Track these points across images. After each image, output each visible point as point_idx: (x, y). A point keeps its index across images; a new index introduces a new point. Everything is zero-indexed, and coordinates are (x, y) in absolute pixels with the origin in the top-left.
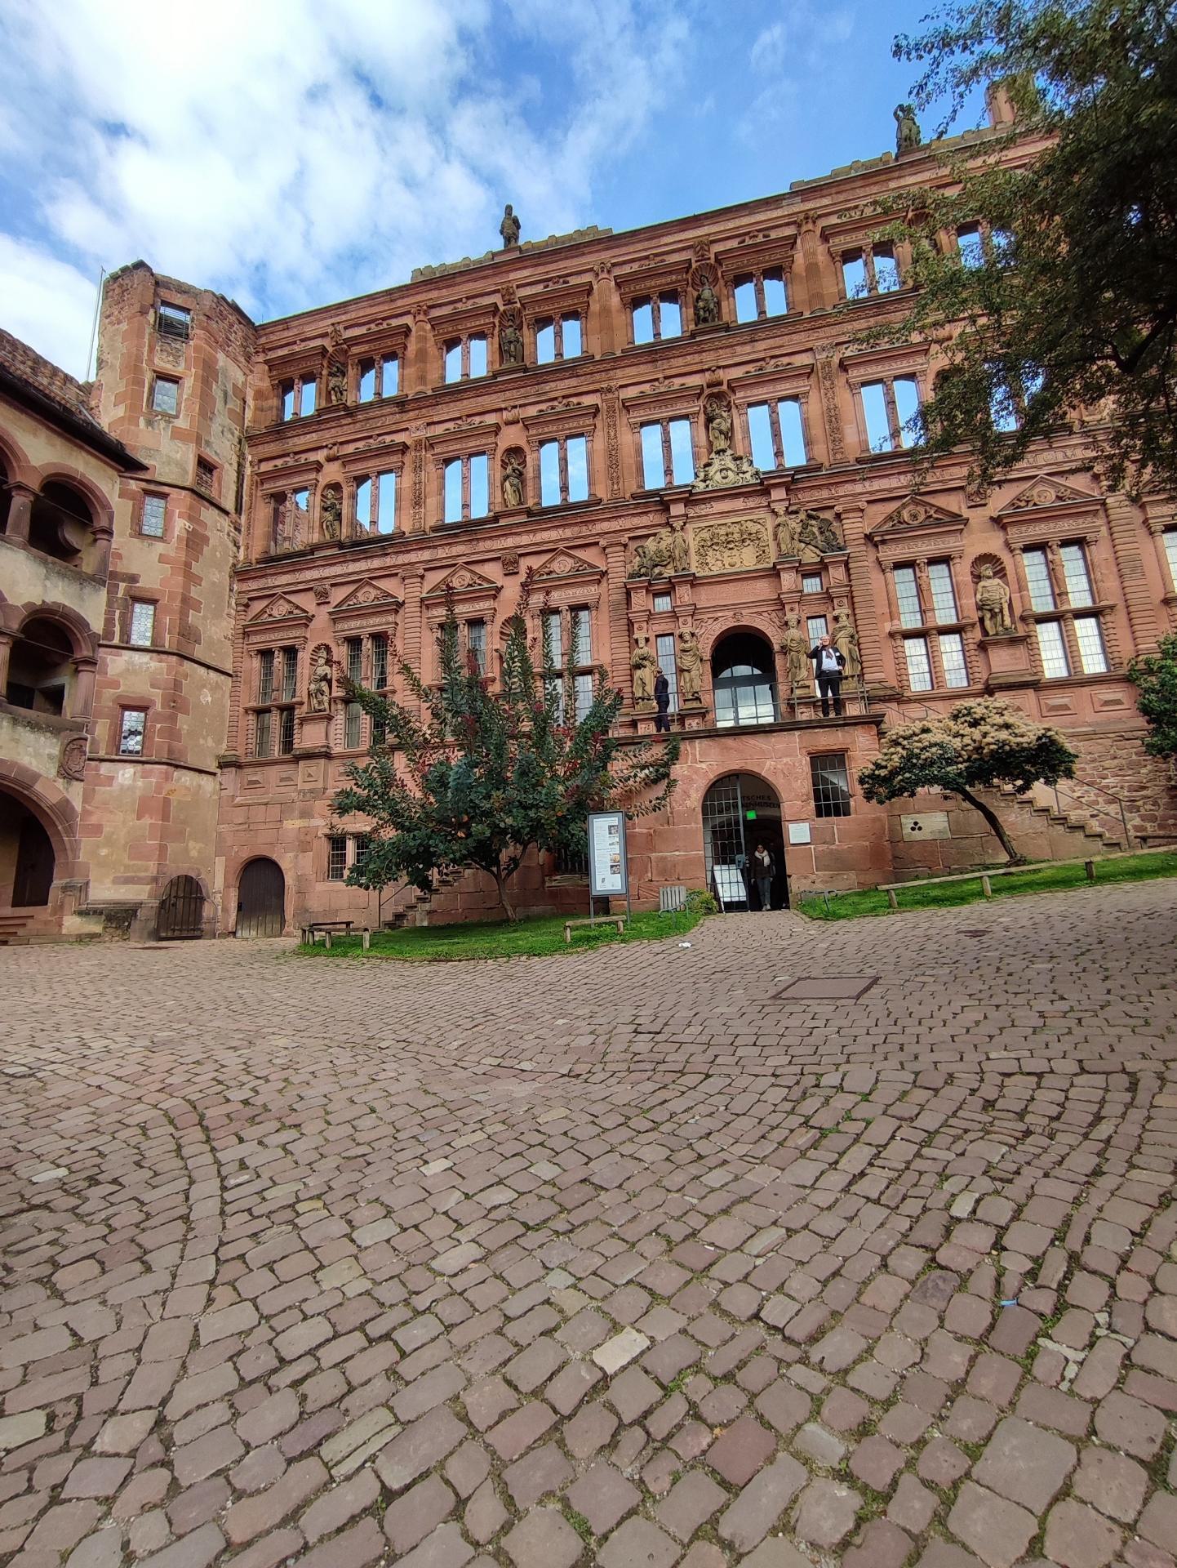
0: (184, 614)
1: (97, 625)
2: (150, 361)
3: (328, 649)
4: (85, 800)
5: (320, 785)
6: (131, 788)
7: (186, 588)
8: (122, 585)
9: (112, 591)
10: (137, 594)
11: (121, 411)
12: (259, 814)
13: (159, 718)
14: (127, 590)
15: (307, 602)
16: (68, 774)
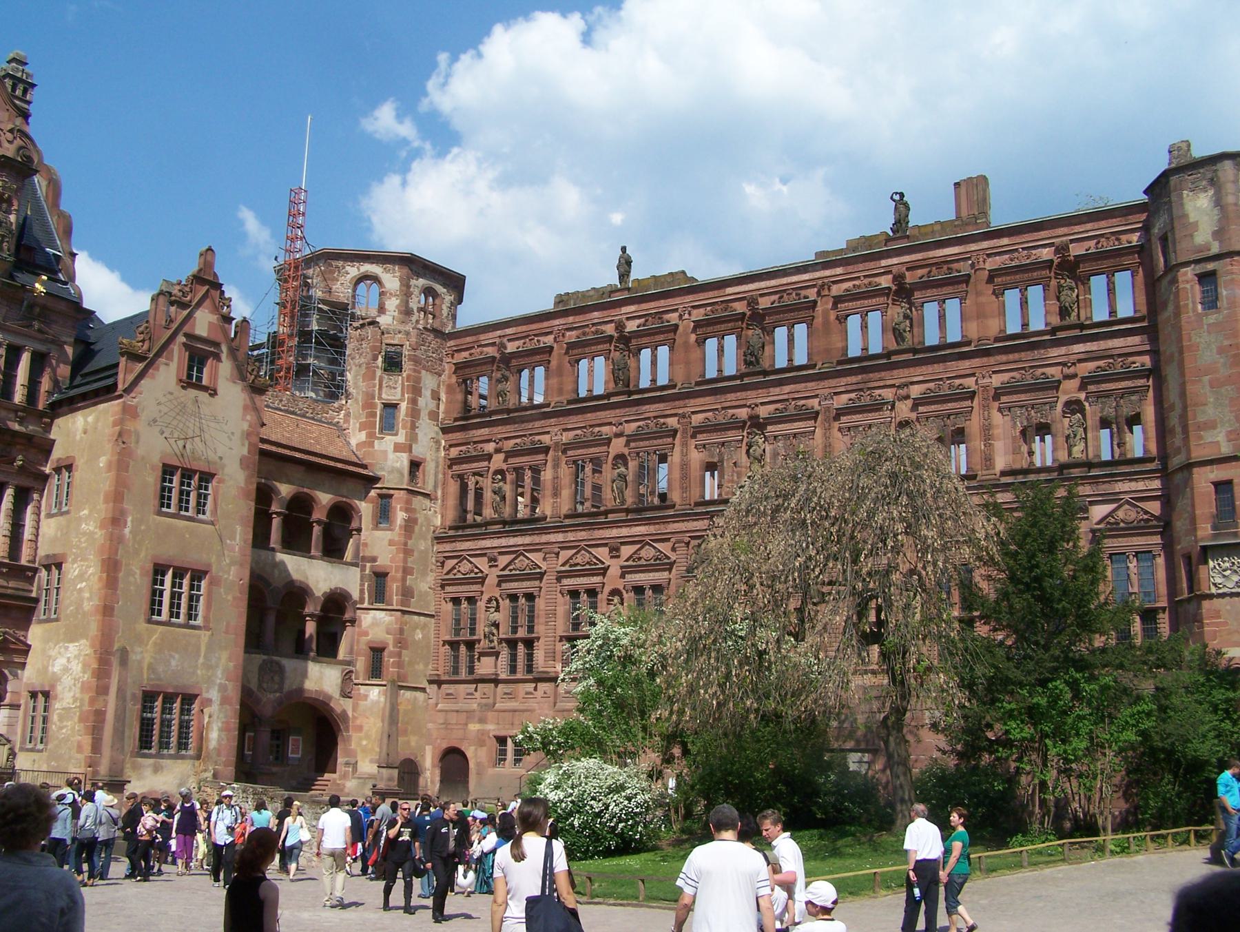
0: (404, 580)
1: (356, 595)
2: (380, 398)
3: (497, 600)
4: (354, 710)
5: (491, 701)
6: (378, 702)
7: (405, 561)
8: (368, 565)
9: (363, 570)
10: (378, 570)
11: (362, 436)
12: (453, 718)
13: (391, 655)
14: (372, 567)
15: (482, 563)
16: (346, 695)
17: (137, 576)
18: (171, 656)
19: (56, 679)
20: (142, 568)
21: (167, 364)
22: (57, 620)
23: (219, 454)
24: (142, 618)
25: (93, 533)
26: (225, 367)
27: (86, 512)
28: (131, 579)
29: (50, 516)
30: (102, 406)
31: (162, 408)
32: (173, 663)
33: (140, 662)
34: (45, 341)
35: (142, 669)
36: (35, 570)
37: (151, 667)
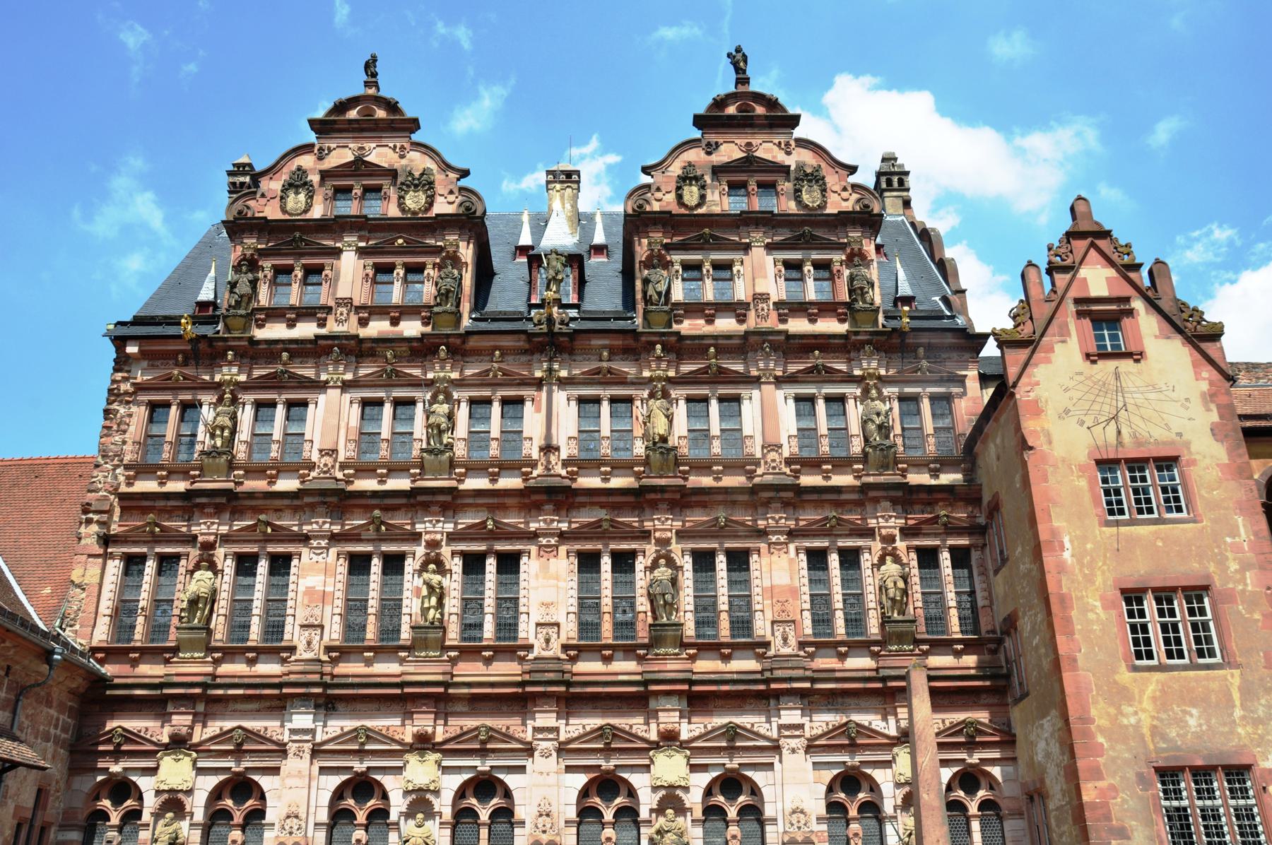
17: (1100, 610)
18: (1185, 712)
19: (1043, 771)
20: (1102, 598)
21: (1063, 342)
22: (1027, 694)
23: (1175, 430)
24: (1123, 667)
25: (1030, 571)
26: (1146, 323)
27: (1019, 549)
28: (1091, 616)
29: (996, 572)
30: (1002, 419)
31: (1068, 394)
32: (1192, 722)
33: (1137, 727)
34: (940, 382)
35: (1142, 737)
36: (1000, 642)
37: (1154, 729)
